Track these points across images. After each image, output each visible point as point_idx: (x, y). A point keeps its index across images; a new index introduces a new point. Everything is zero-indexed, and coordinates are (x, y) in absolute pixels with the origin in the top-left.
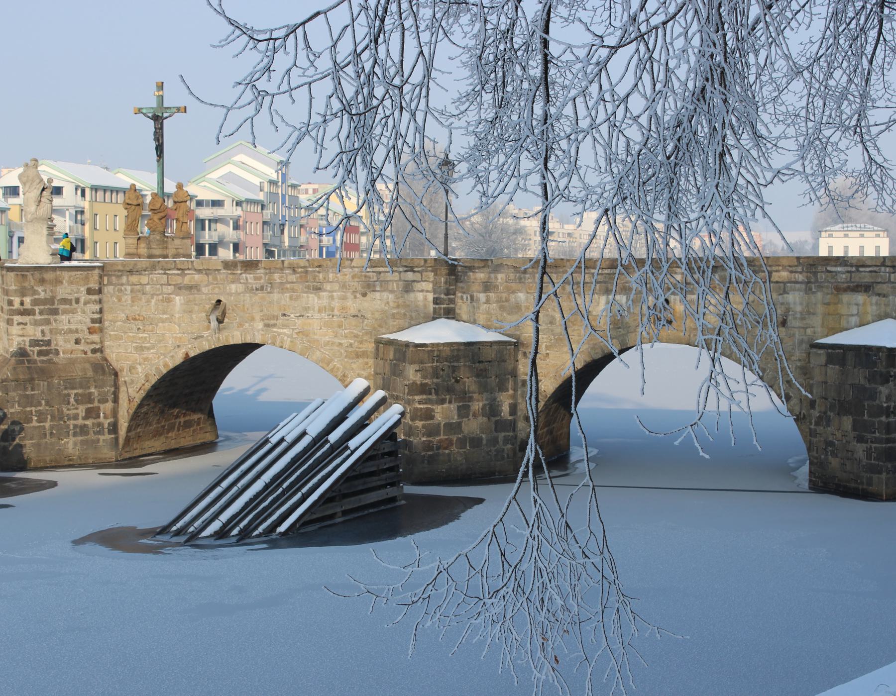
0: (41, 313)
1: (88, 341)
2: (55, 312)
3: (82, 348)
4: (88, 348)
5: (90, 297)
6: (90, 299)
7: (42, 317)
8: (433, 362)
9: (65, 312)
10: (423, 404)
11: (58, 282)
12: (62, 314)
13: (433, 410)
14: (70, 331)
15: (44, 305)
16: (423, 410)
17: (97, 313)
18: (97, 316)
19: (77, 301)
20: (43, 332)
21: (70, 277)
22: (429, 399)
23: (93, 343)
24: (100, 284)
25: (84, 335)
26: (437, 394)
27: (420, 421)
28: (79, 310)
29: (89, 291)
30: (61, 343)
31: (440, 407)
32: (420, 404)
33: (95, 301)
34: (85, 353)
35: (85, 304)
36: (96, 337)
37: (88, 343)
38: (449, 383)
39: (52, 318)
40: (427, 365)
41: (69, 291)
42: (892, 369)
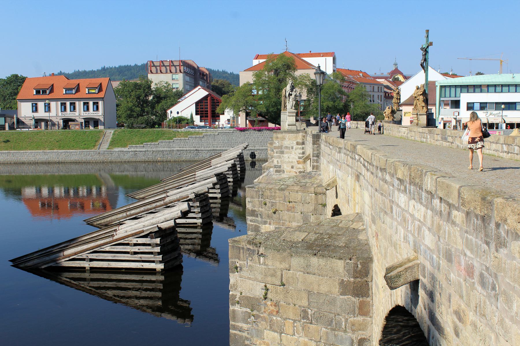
0: (277, 153)
1: (297, 167)
2: (282, 153)
3: (295, 170)
4: (298, 171)
5: (298, 146)
6: (298, 147)
7: (277, 155)
8: (259, 198)
9: (287, 153)
10: (253, 222)
11: (284, 139)
12: (286, 154)
13: (259, 227)
14: (289, 162)
15: (278, 149)
16: (254, 226)
17: (301, 154)
18: (301, 155)
19: (292, 148)
20: (278, 161)
21: (289, 136)
22: (257, 220)
23: (300, 168)
24: (303, 140)
25: (295, 164)
26: (261, 217)
27: (252, 232)
28: (293, 152)
29: (298, 144)
30: (285, 167)
31: (263, 226)
32: (251, 222)
33: (300, 148)
34: (296, 173)
35: (296, 149)
36: (301, 166)
37: (297, 168)
38: (269, 212)
39: (282, 155)
40: (255, 199)
41: (289, 143)
42: (237, 260)
